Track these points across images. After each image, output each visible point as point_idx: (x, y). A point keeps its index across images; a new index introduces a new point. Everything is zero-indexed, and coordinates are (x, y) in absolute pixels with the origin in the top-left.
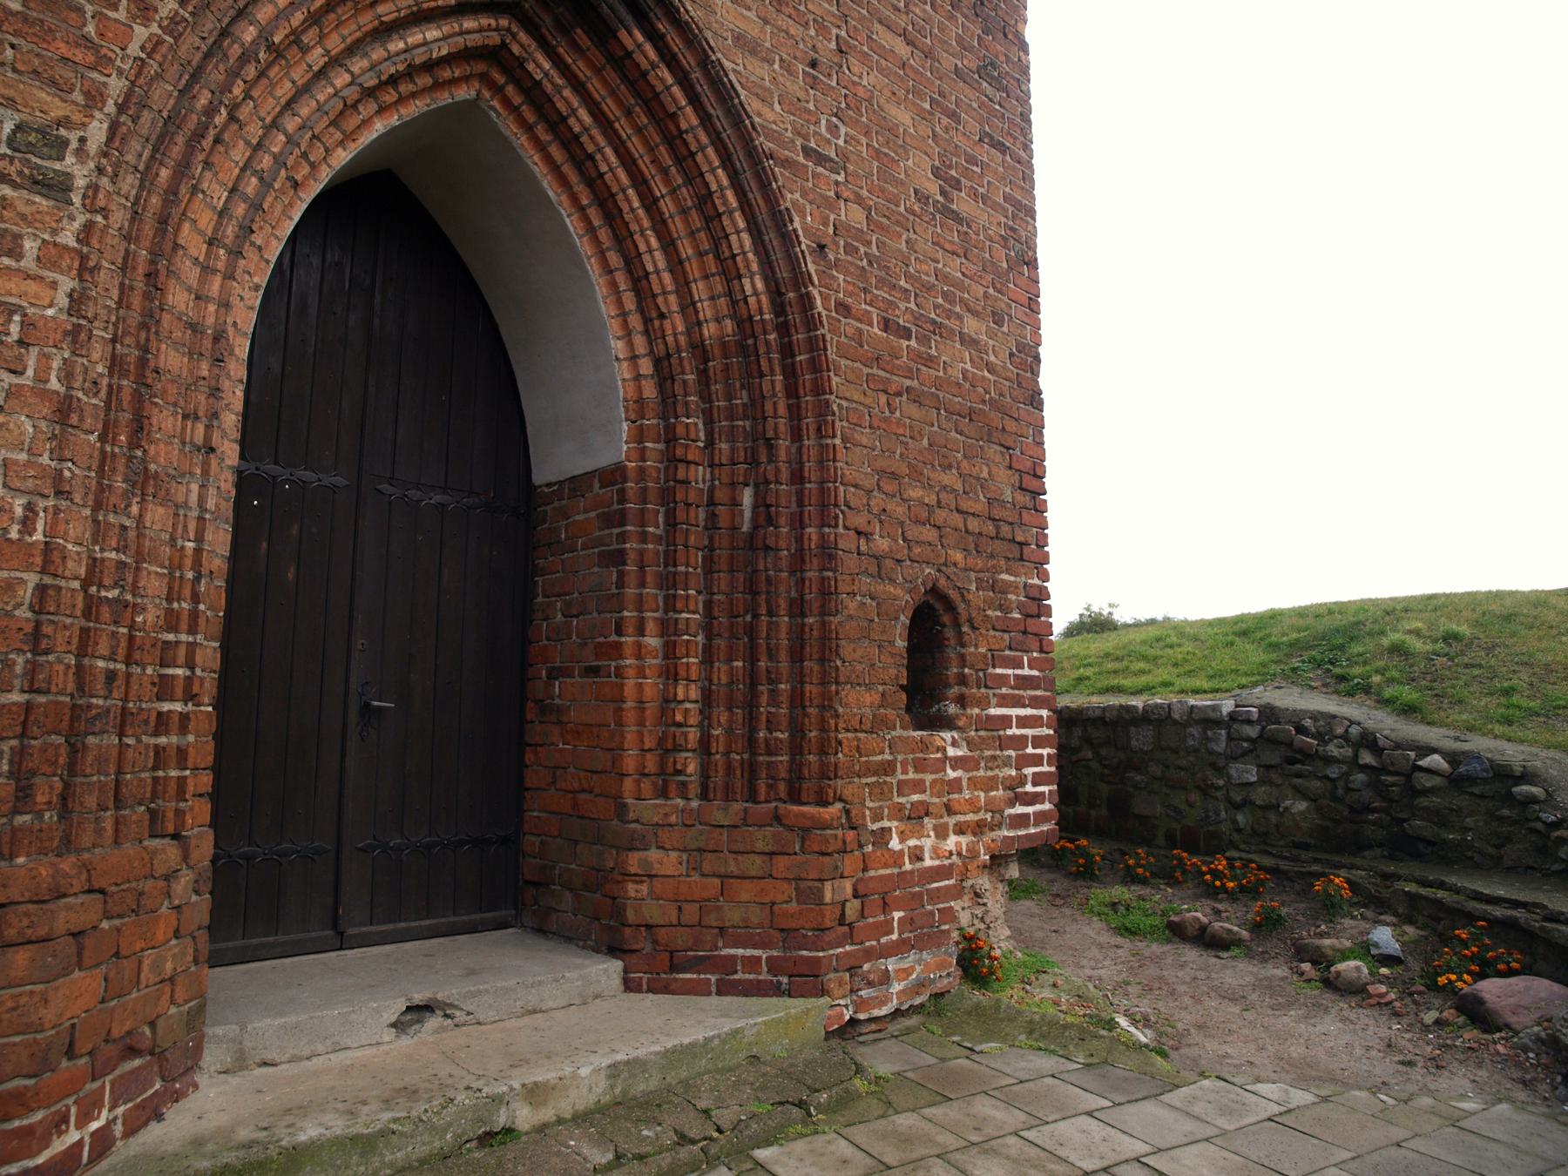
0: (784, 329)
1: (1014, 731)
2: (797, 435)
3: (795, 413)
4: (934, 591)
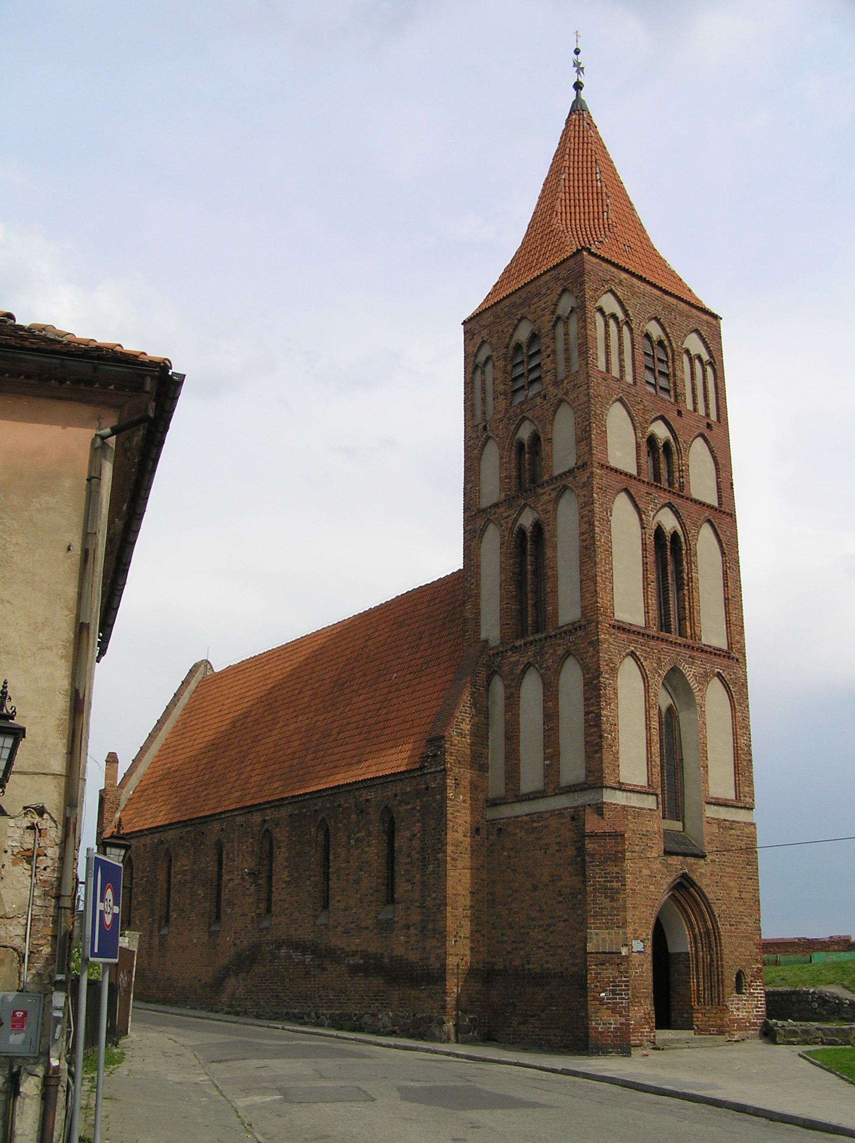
0: (714, 929)
1: (756, 995)
2: (716, 947)
3: (716, 943)
4: (740, 971)
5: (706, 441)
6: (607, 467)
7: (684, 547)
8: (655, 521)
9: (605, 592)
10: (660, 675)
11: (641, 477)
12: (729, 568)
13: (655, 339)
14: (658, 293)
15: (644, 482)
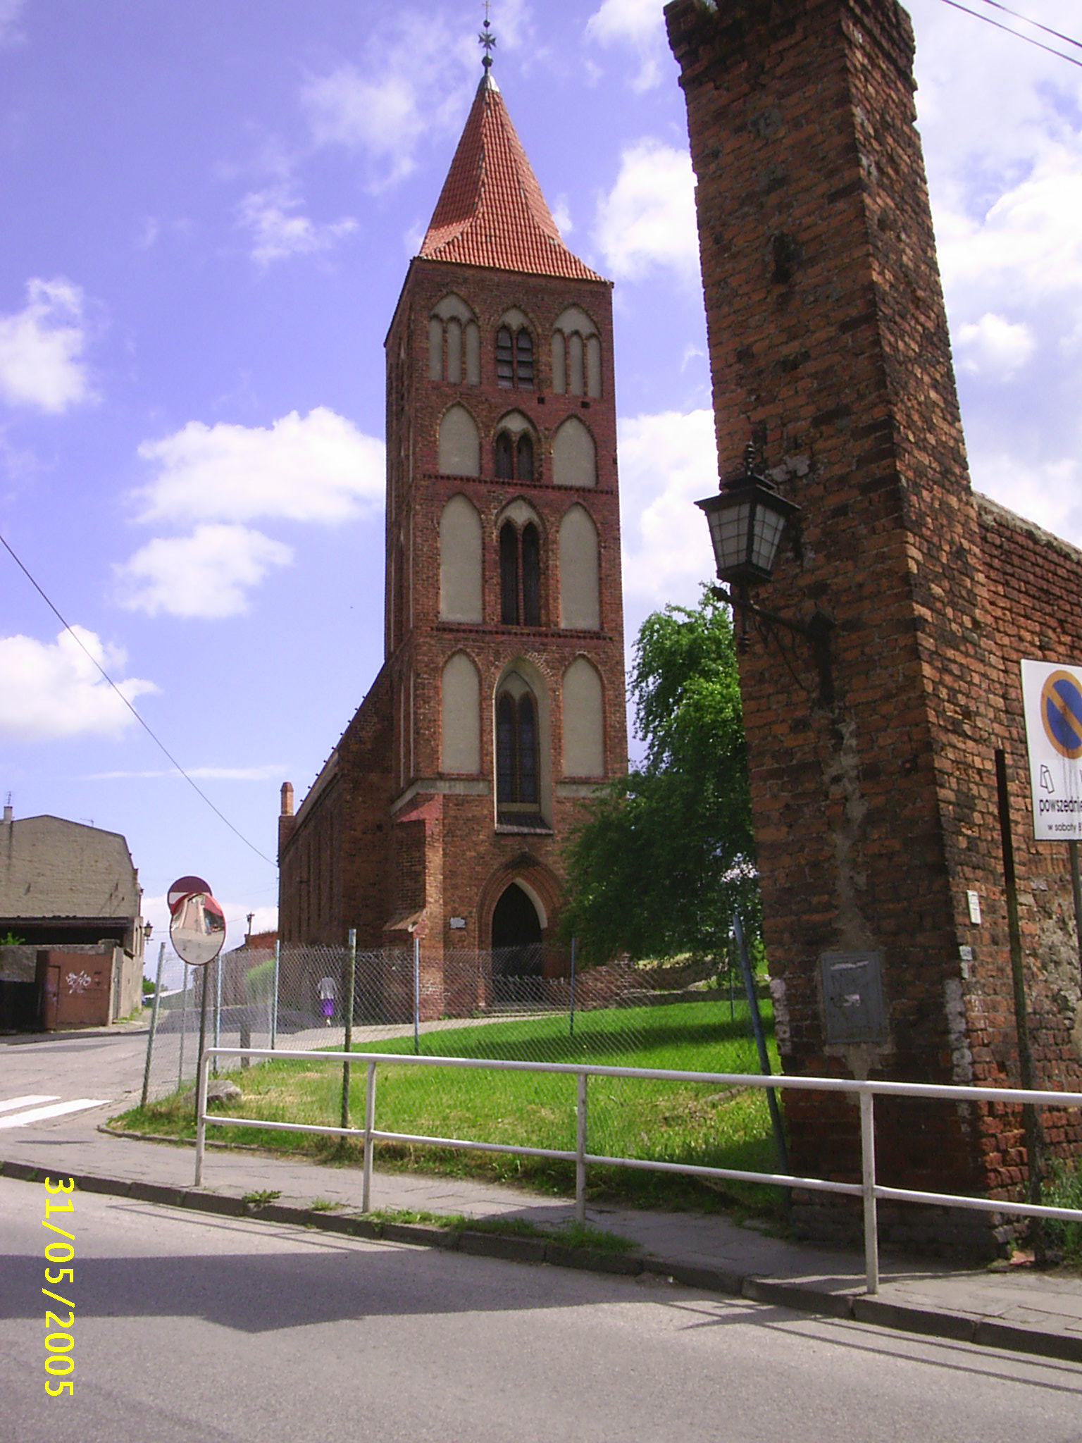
5: (580, 420)
6: (436, 477)
7: (542, 536)
8: (503, 517)
9: (428, 598)
10: (497, 667)
11: (483, 478)
12: (605, 547)
13: (514, 328)
14: (519, 279)
15: (486, 482)
